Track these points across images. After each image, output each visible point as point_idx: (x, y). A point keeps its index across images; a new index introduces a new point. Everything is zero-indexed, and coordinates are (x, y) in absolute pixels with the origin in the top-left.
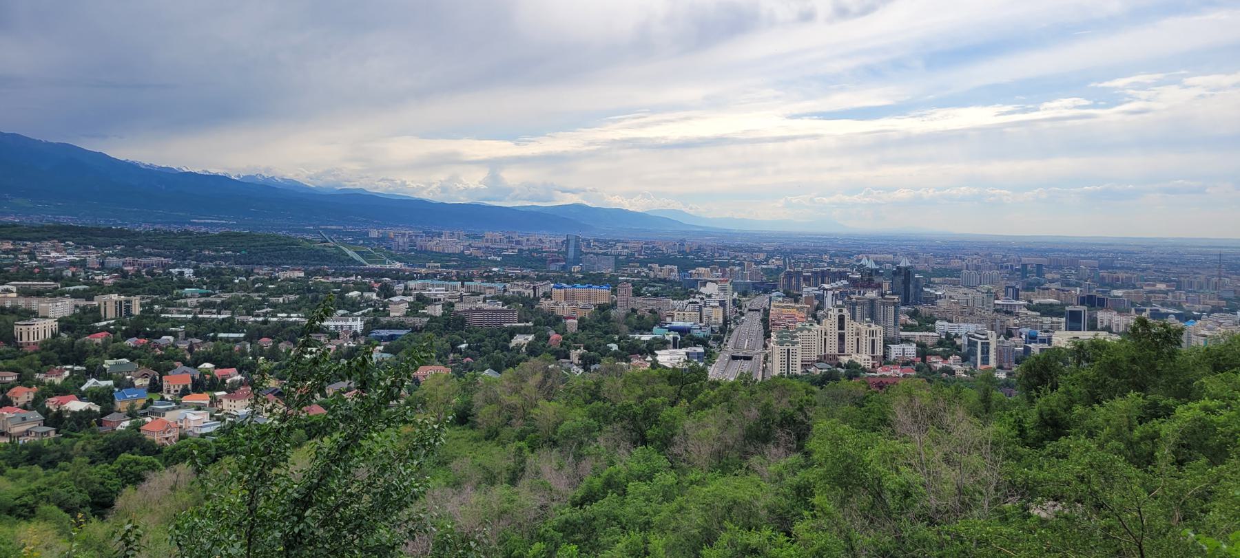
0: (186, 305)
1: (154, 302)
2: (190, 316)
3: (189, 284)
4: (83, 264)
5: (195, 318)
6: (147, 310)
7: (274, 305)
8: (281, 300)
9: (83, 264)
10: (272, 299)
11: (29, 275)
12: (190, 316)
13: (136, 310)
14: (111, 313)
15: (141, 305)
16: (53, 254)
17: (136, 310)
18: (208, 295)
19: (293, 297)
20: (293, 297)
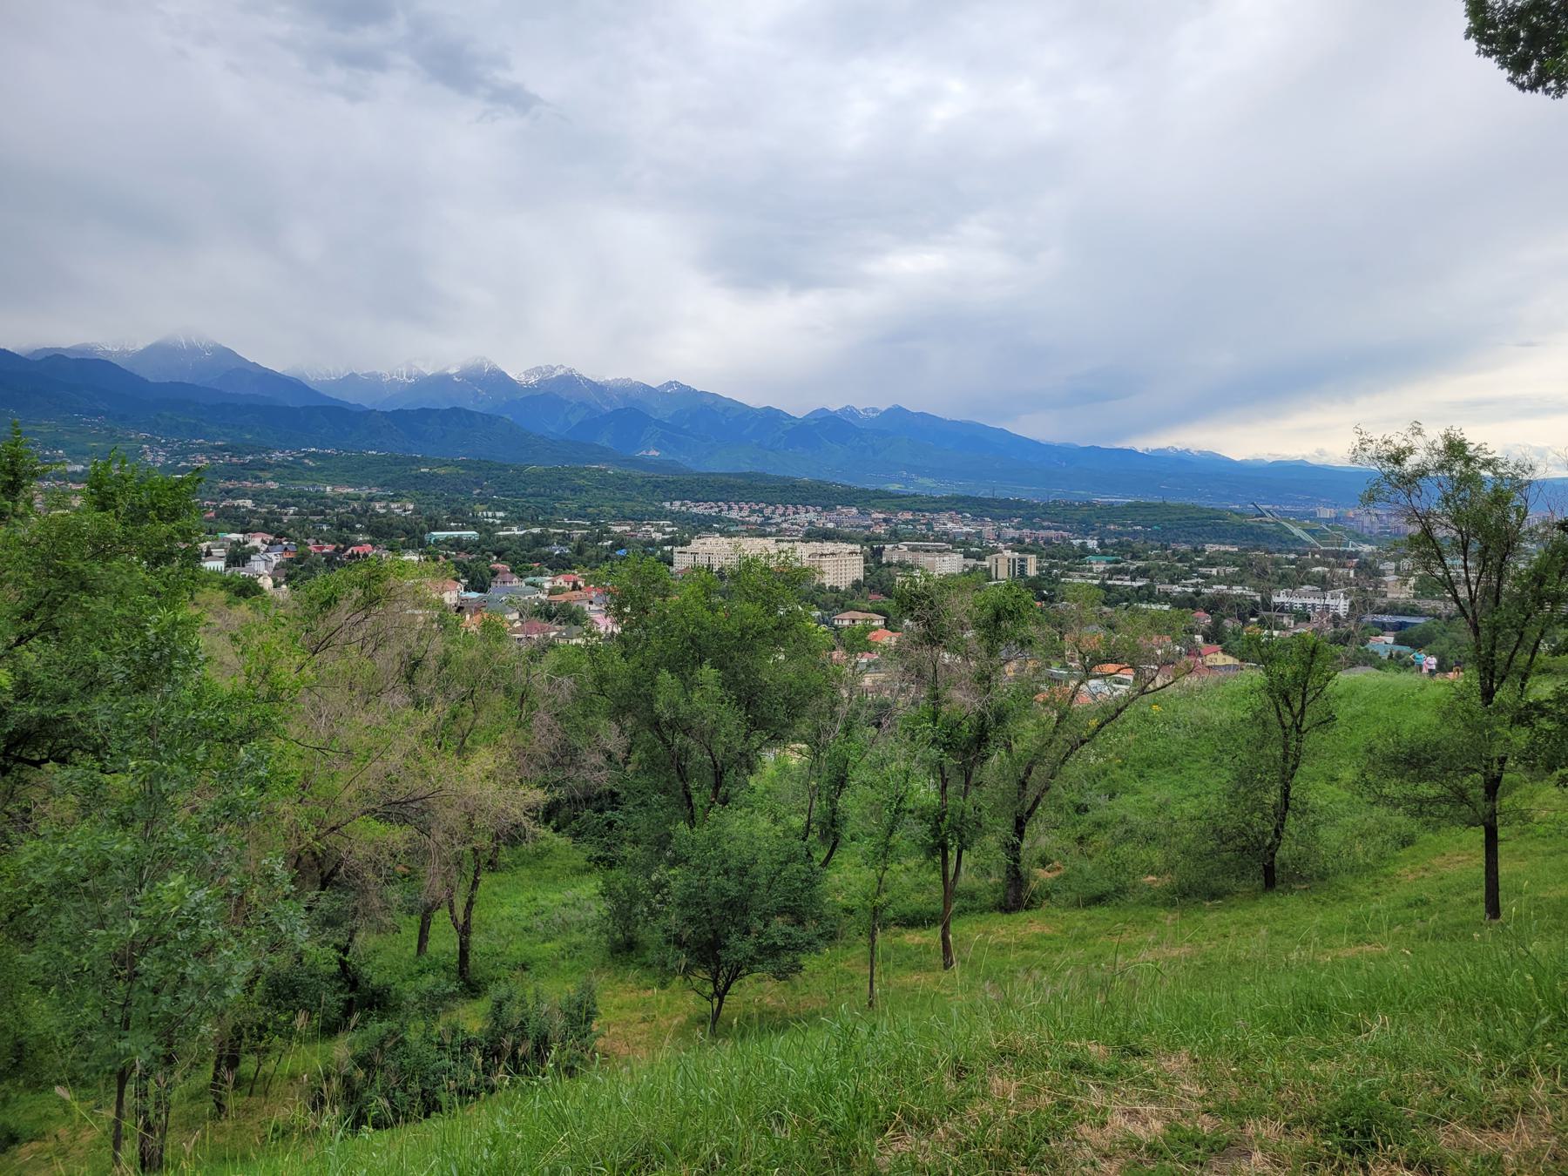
0: (1091, 570)
1: (1052, 566)
2: (1096, 582)
3: (1093, 552)
4: (979, 534)
5: (1103, 586)
6: (1045, 575)
7: (1205, 576)
8: (1214, 572)
9: (979, 534)
10: (1203, 570)
11: (924, 538)
12: (1096, 582)
13: (1032, 571)
14: (1003, 573)
15: (1038, 569)
16: (950, 525)
17: (1032, 571)
18: (1117, 562)
19: (1230, 570)
20: (1230, 570)
